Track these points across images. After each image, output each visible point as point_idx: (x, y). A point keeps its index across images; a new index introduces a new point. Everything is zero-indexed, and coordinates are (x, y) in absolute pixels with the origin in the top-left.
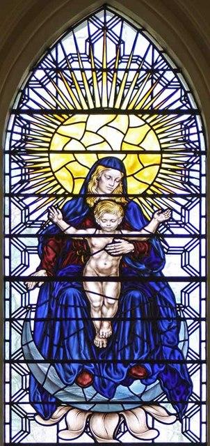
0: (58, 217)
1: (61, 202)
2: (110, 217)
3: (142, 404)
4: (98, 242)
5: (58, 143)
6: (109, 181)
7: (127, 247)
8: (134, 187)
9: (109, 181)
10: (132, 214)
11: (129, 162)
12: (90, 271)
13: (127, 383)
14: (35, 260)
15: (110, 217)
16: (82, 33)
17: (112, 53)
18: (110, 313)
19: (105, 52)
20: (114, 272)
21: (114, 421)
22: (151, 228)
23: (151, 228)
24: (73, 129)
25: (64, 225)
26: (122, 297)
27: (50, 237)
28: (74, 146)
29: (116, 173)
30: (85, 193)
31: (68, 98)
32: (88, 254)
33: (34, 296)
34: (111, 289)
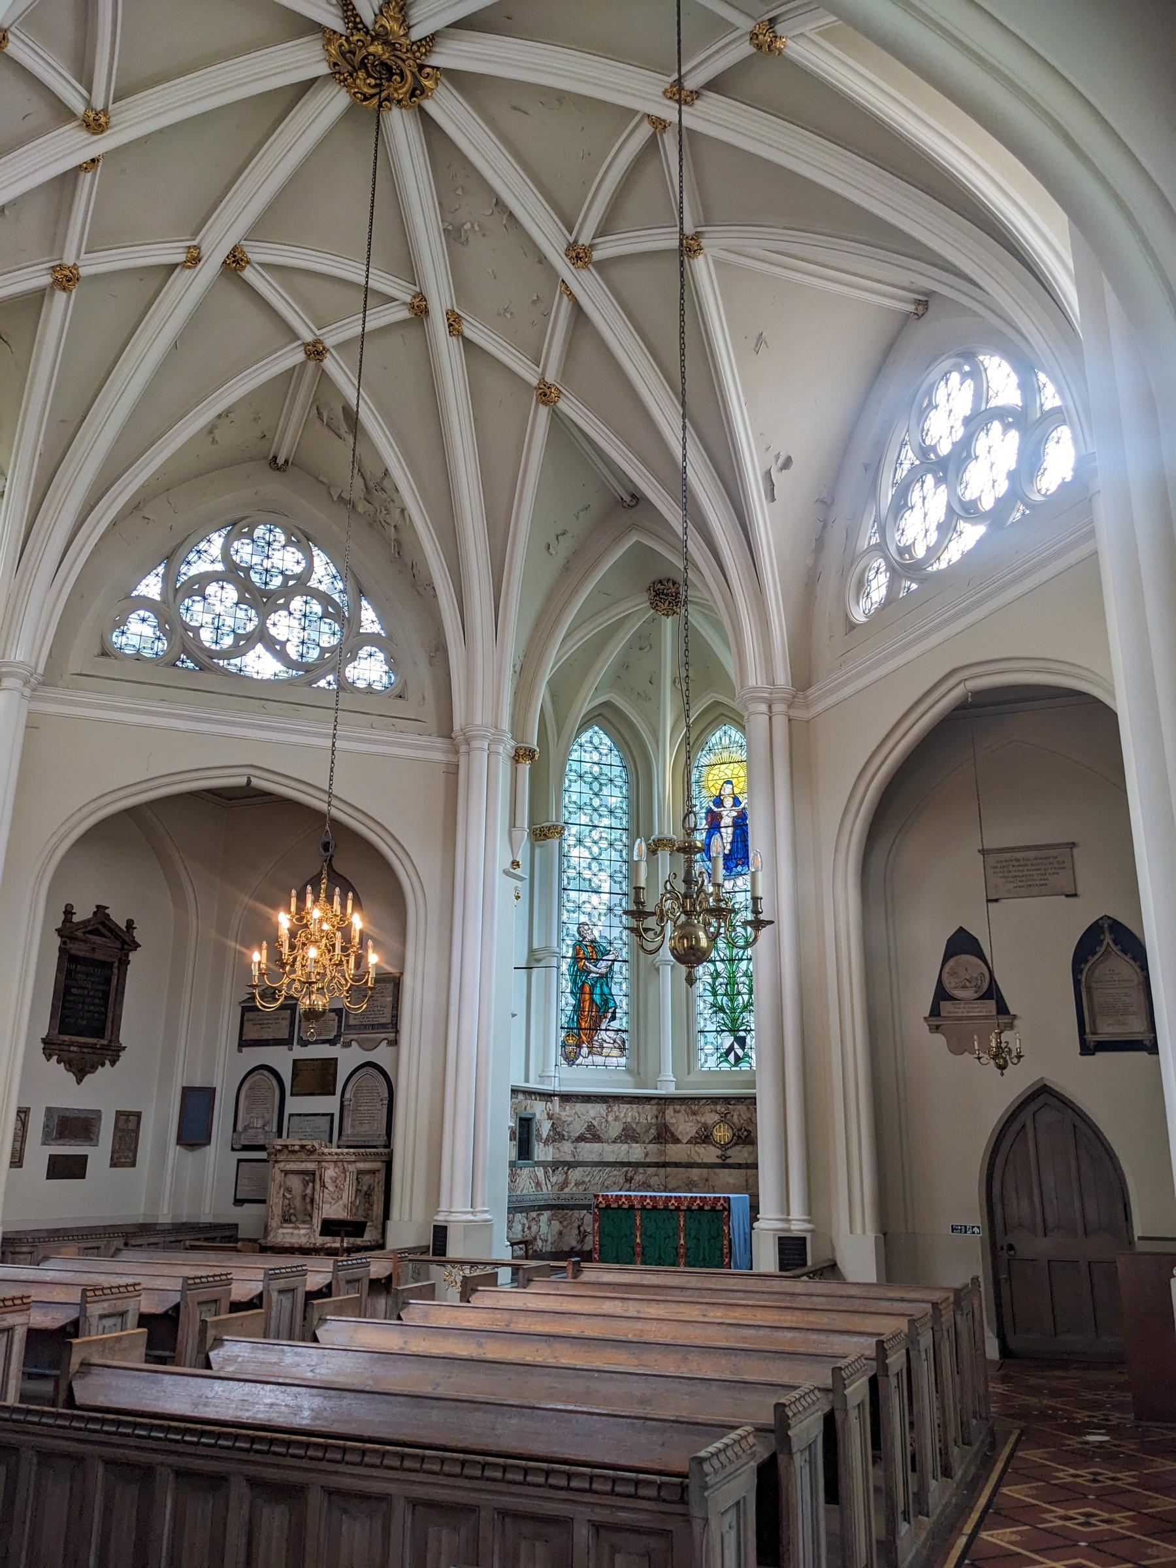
0: (711, 805)
1: (712, 799)
2: (728, 802)
3: (742, 875)
4: (724, 813)
5: (711, 777)
6: (728, 789)
7: (735, 814)
8: (737, 791)
9: (728, 789)
10: (736, 802)
11: (734, 781)
12: (722, 825)
13: (736, 867)
14: (704, 822)
15: (728, 802)
16: (717, 735)
17: (728, 742)
18: (730, 840)
19: (725, 741)
20: (731, 824)
21: (732, 882)
22: (742, 806)
23: (742, 806)
24: (715, 771)
25: (713, 807)
26: (734, 834)
27: (709, 811)
28: (716, 778)
29: (730, 786)
30: (720, 795)
31: (712, 759)
32: (722, 818)
33: (705, 834)
34: (730, 830)
